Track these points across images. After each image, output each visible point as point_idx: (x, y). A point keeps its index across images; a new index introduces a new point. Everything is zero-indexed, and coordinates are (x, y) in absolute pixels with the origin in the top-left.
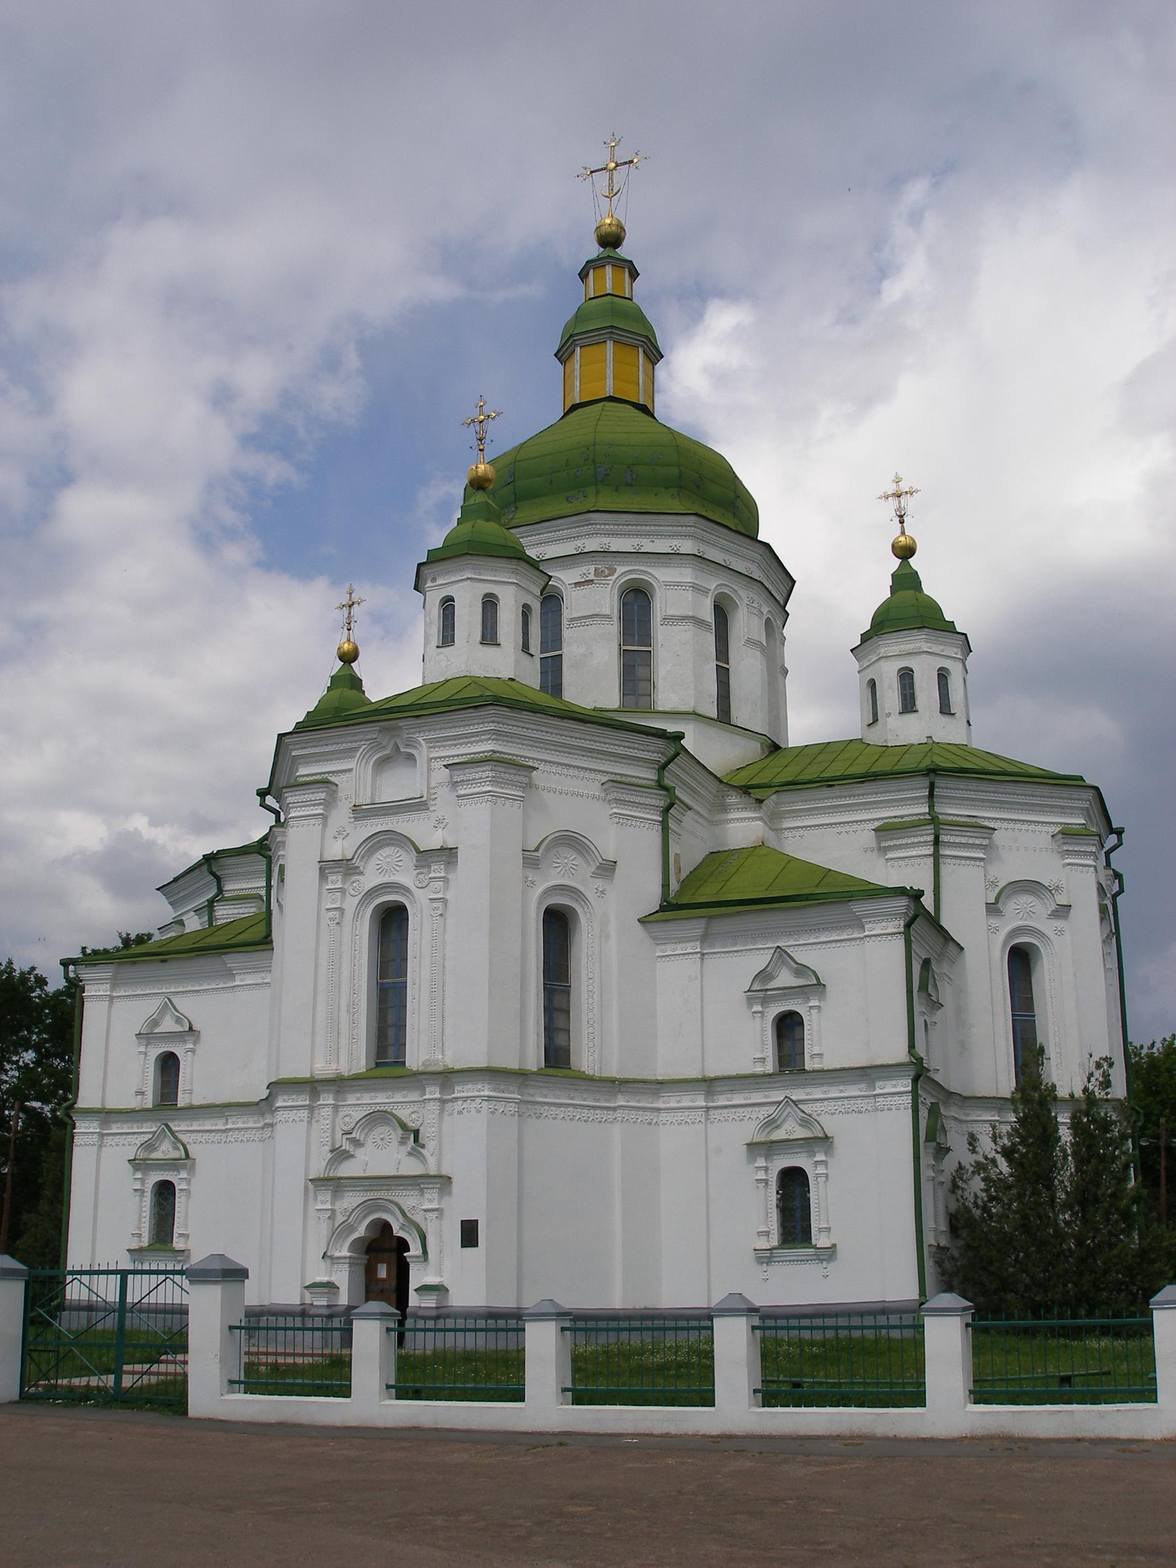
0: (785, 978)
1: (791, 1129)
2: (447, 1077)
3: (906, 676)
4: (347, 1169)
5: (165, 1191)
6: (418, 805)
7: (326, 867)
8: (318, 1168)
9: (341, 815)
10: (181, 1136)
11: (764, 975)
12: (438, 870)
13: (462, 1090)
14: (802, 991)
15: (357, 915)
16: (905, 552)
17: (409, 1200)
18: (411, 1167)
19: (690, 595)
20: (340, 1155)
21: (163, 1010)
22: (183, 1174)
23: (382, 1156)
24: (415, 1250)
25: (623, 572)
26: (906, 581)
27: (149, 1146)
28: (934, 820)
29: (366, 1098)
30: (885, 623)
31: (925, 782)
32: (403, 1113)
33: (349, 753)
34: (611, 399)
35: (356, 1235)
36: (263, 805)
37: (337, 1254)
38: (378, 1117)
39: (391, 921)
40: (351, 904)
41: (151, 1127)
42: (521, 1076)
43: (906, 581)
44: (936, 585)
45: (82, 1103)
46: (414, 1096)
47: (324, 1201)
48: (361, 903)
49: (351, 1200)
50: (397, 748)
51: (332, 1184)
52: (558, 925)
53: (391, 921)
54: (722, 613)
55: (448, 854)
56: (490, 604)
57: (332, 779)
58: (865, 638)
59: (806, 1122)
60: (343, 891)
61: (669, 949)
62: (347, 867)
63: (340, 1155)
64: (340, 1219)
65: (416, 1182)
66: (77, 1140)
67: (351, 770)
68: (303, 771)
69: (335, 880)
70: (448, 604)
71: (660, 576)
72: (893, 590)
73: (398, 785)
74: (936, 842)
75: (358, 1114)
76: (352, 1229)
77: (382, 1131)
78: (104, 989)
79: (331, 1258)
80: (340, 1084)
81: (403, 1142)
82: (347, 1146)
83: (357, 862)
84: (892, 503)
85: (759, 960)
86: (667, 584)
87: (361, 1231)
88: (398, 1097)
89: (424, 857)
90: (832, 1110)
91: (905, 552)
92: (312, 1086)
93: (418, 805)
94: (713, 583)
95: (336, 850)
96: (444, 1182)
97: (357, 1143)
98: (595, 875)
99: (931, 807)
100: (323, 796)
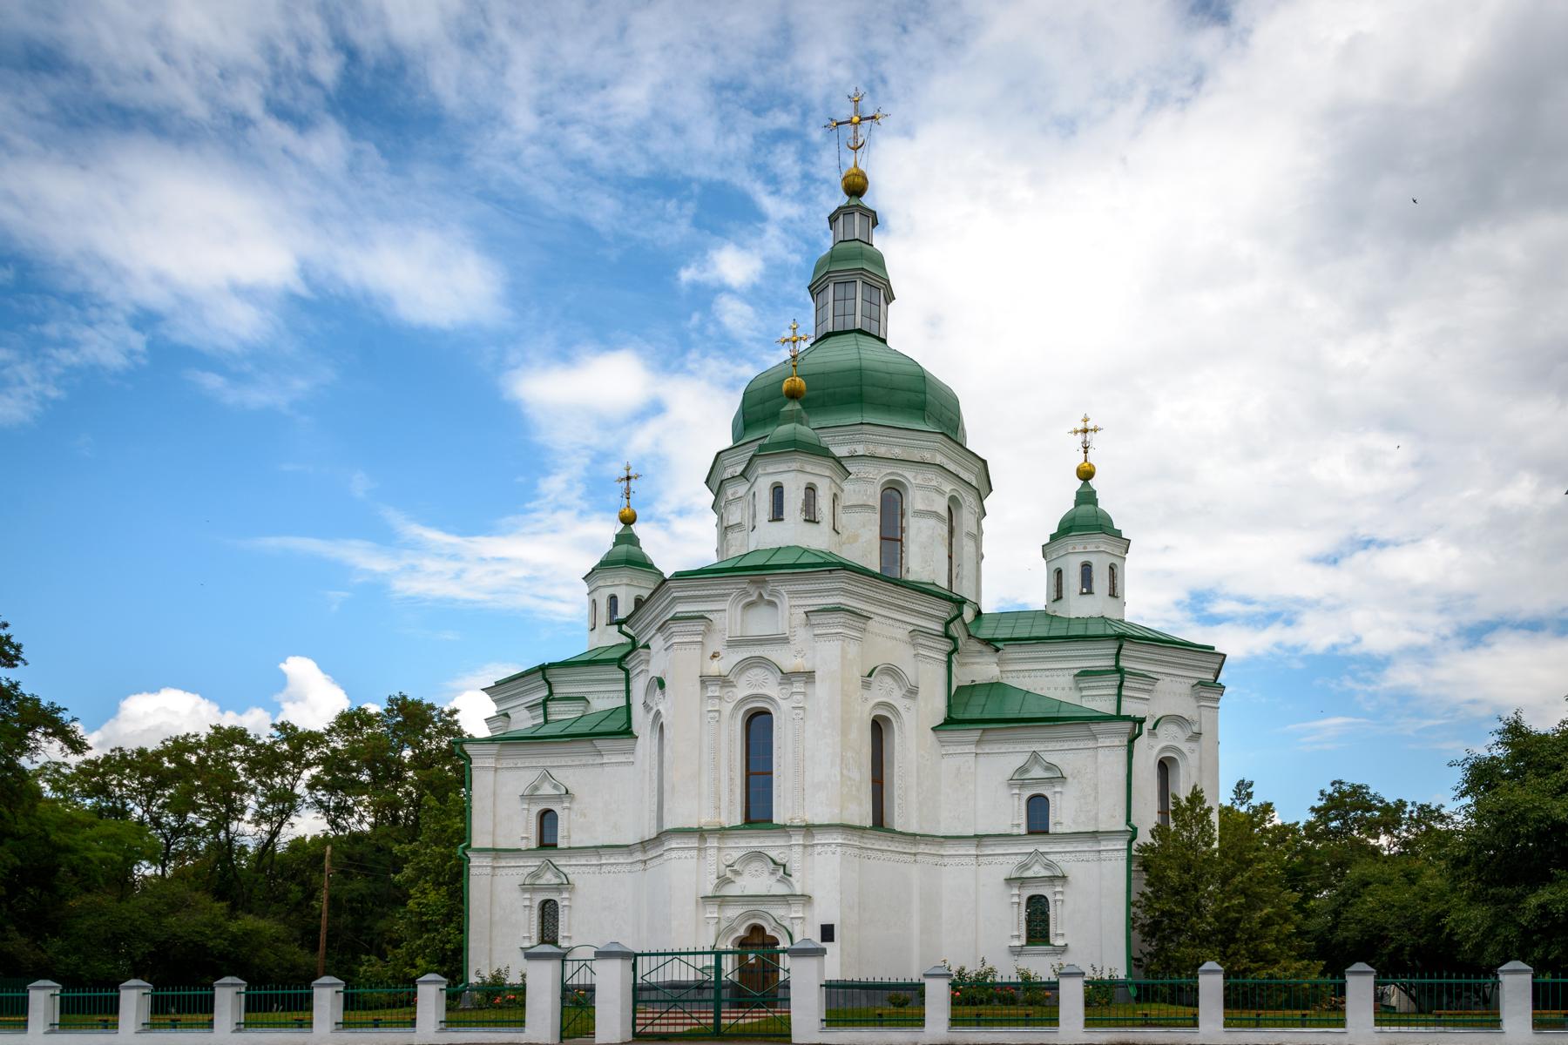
0: (1037, 772)
1: (1037, 870)
2: (809, 829)
3: (1087, 569)
4: (730, 890)
8: (709, 891)
11: (1023, 770)
12: (798, 687)
13: (820, 838)
14: (1050, 781)
15: (732, 716)
16: (1086, 475)
17: (778, 911)
18: (781, 889)
20: (723, 881)
23: (757, 881)
26: (1086, 497)
28: (1119, 670)
30: (1068, 528)
31: (1115, 645)
32: (773, 854)
34: (860, 331)
36: (620, 631)
38: (758, 855)
39: (758, 723)
40: (727, 708)
42: (864, 829)
43: (1086, 497)
44: (1108, 502)
45: (475, 845)
46: (781, 842)
47: (712, 912)
48: (736, 708)
49: (733, 912)
50: (761, 595)
51: (720, 900)
52: (879, 728)
53: (758, 723)
55: (809, 676)
58: (1053, 538)
59: (1048, 866)
60: (720, 698)
61: (951, 749)
62: (724, 681)
64: (724, 924)
65: (785, 899)
69: (714, 690)
70: (778, 491)
71: (910, 476)
72: (1077, 503)
73: (761, 623)
74: (1120, 687)
75: (736, 855)
76: (734, 930)
77: (756, 865)
78: (490, 762)
80: (723, 832)
81: (773, 873)
82: (729, 875)
83: (731, 678)
84: (1080, 437)
85: (1020, 760)
87: (741, 932)
88: (768, 842)
89: (788, 677)
90: (1063, 857)
91: (1086, 475)
92: (701, 833)
94: (948, 487)
95: (715, 668)
96: (806, 899)
97: (737, 873)
98: (904, 696)
99: (1117, 661)
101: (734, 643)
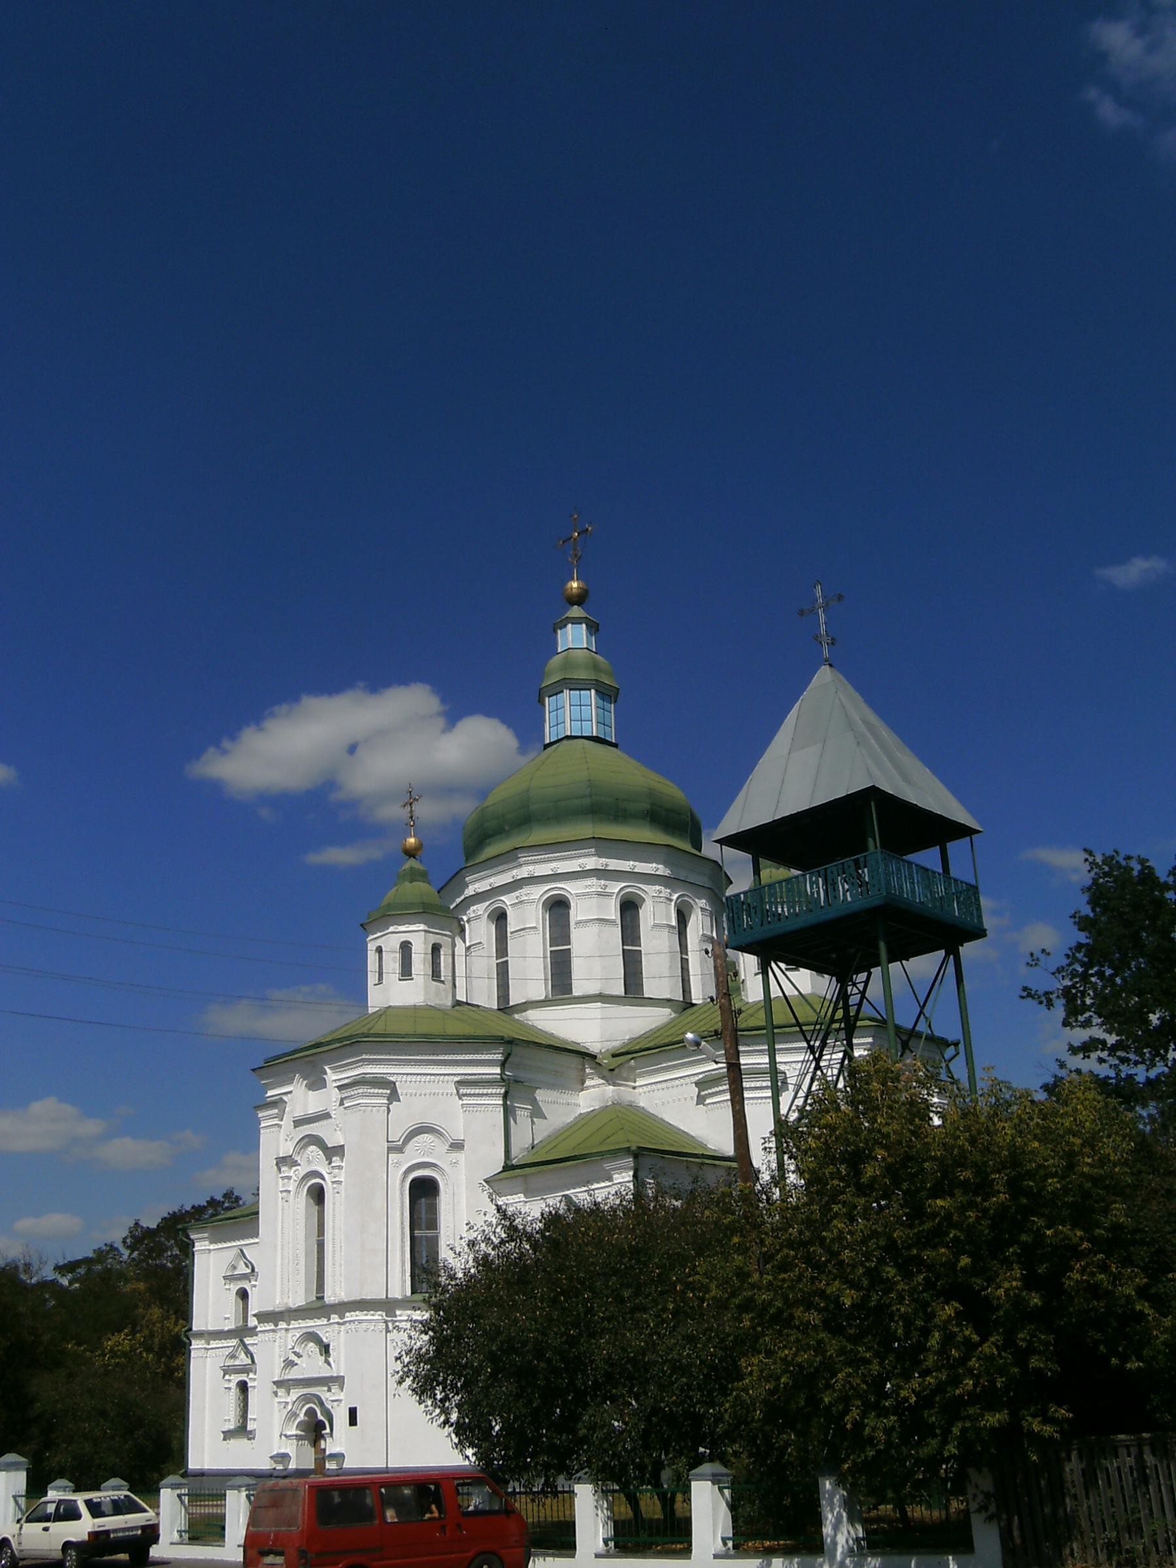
4: (294, 1374)
5: (243, 1387)
6: (326, 1116)
7: (284, 1161)
9: (287, 1123)
10: (250, 1348)
12: (336, 1161)
15: (297, 1193)
18: (325, 1372)
19: (595, 901)
20: (290, 1364)
21: (236, 1258)
22: (251, 1375)
23: (311, 1365)
24: (328, 1430)
25: (538, 893)
27: (233, 1356)
29: (303, 1324)
33: (290, 1081)
37: (289, 1433)
40: (292, 1187)
41: (234, 1342)
46: (325, 1321)
54: (629, 907)
55: (339, 1151)
56: (406, 947)
57: (285, 1098)
63: (290, 1364)
67: (290, 1092)
68: (270, 1093)
71: (571, 889)
76: (296, 1415)
79: (286, 1436)
82: (293, 1358)
83: (297, 1158)
86: (577, 895)
87: (302, 1417)
88: (319, 1322)
93: (326, 1116)
94: (616, 887)
96: (339, 1380)
97: (299, 1356)
100: (276, 1111)
101: (298, 1123)
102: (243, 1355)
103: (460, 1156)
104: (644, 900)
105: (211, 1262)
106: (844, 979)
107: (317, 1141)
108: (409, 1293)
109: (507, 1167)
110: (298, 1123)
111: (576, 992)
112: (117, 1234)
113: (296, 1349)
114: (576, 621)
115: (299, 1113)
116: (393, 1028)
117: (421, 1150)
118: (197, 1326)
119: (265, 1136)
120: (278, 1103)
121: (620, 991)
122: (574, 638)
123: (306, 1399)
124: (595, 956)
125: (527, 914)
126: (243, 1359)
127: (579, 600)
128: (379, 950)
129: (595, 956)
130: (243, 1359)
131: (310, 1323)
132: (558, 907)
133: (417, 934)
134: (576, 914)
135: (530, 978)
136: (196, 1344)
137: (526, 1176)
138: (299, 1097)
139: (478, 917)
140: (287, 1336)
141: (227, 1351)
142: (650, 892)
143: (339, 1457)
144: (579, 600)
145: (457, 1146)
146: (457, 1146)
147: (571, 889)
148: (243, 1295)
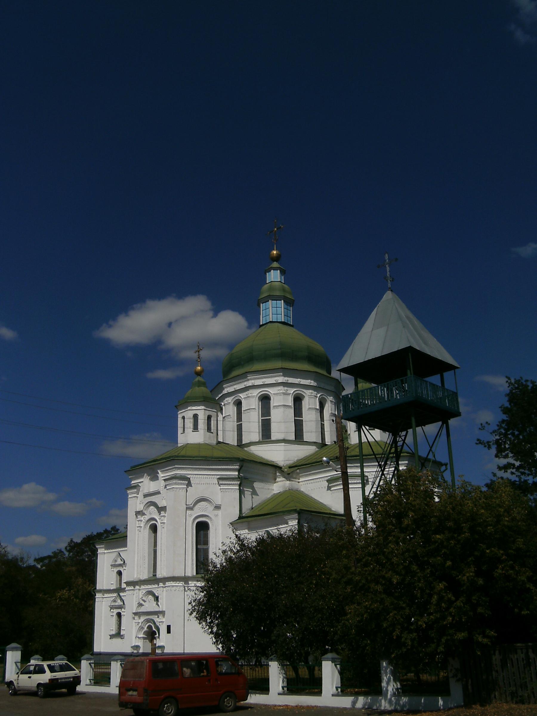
4: (142, 609)
5: (119, 615)
6: (158, 493)
7: (139, 513)
9: (141, 495)
10: (122, 597)
12: (163, 513)
15: (145, 527)
18: (156, 609)
19: (282, 397)
20: (140, 605)
22: (123, 610)
23: (150, 605)
25: (256, 393)
27: (115, 601)
33: (142, 477)
35: (144, 630)
37: (140, 636)
41: (115, 595)
46: (156, 586)
54: (298, 400)
55: (164, 509)
56: (196, 417)
57: (140, 484)
63: (140, 605)
66: (96, 600)
67: (142, 482)
68: (133, 482)
71: (271, 391)
76: (143, 628)
79: (138, 637)
82: (143, 603)
83: (145, 512)
86: (274, 394)
87: (146, 629)
88: (154, 586)
93: (158, 493)
94: (292, 391)
96: (163, 613)
100: (136, 490)
101: (145, 496)
102: (119, 601)
103: (219, 512)
104: (304, 397)
105: (105, 558)
106: (395, 433)
107: (154, 504)
108: (195, 574)
109: (240, 517)
110: (145, 496)
111: (273, 438)
112: (63, 545)
113: (143, 598)
114: (275, 269)
115: (146, 491)
116: (189, 453)
117: (201, 509)
118: (99, 587)
119: (130, 502)
120: (137, 487)
121: (292, 437)
122: (274, 276)
123: (148, 621)
124: (282, 422)
125: (251, 402)
126: (119, 602)
127: (277, 259)
128: (183, 418)
129: (282, 422)
130: (119, 602)
131: (150, 587)
132: (265, 399)
133: (201, 411)
134: (274, 402)
135: (252, 432)
136: (98, 595)
137: (249, 521)
138: (146, 484)
139: (229, 403)
140: (140, 592)
141: (112, 599)
142: (307, 393)
143: (162, 647)
144: (277, 259)
145: (218, 507)
146: (218, 507)
147: (271, 391)
148: (120, 573)
